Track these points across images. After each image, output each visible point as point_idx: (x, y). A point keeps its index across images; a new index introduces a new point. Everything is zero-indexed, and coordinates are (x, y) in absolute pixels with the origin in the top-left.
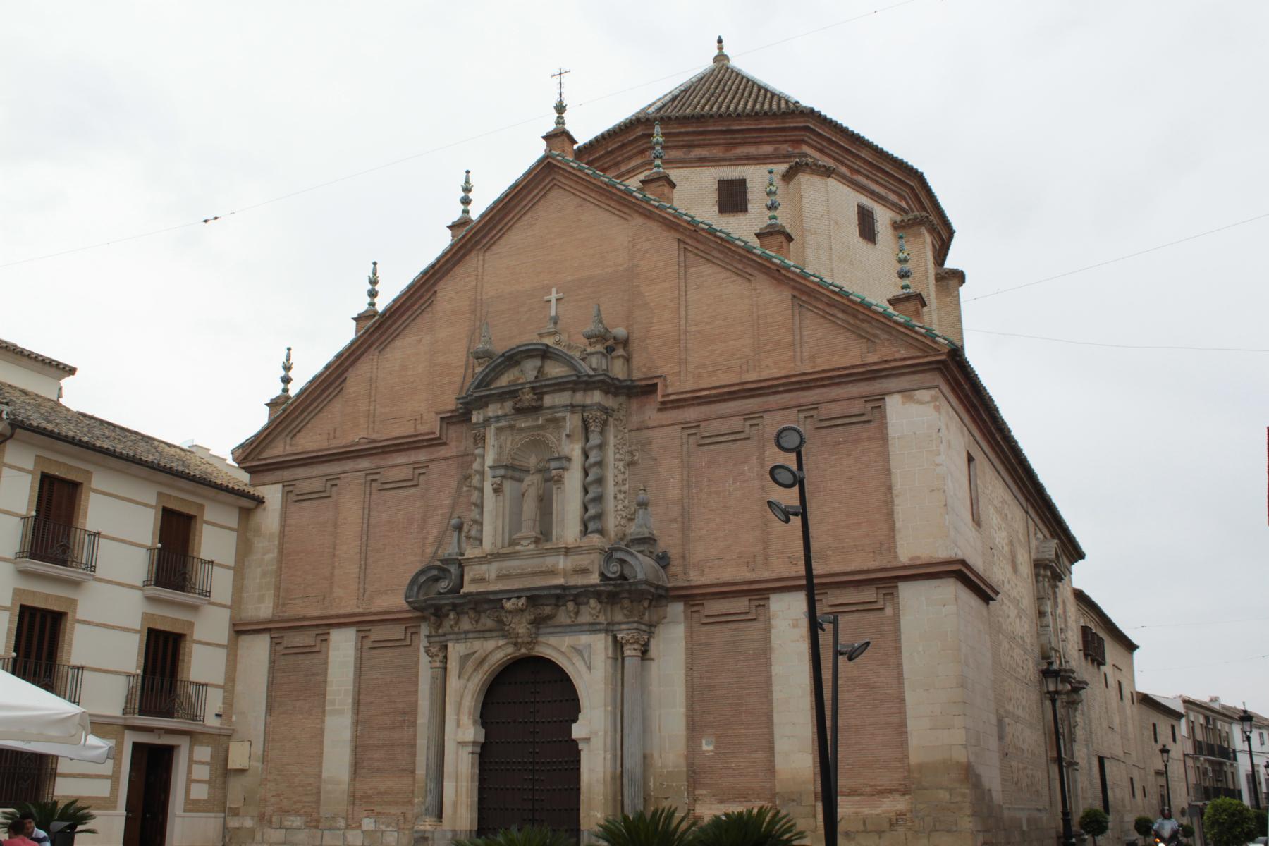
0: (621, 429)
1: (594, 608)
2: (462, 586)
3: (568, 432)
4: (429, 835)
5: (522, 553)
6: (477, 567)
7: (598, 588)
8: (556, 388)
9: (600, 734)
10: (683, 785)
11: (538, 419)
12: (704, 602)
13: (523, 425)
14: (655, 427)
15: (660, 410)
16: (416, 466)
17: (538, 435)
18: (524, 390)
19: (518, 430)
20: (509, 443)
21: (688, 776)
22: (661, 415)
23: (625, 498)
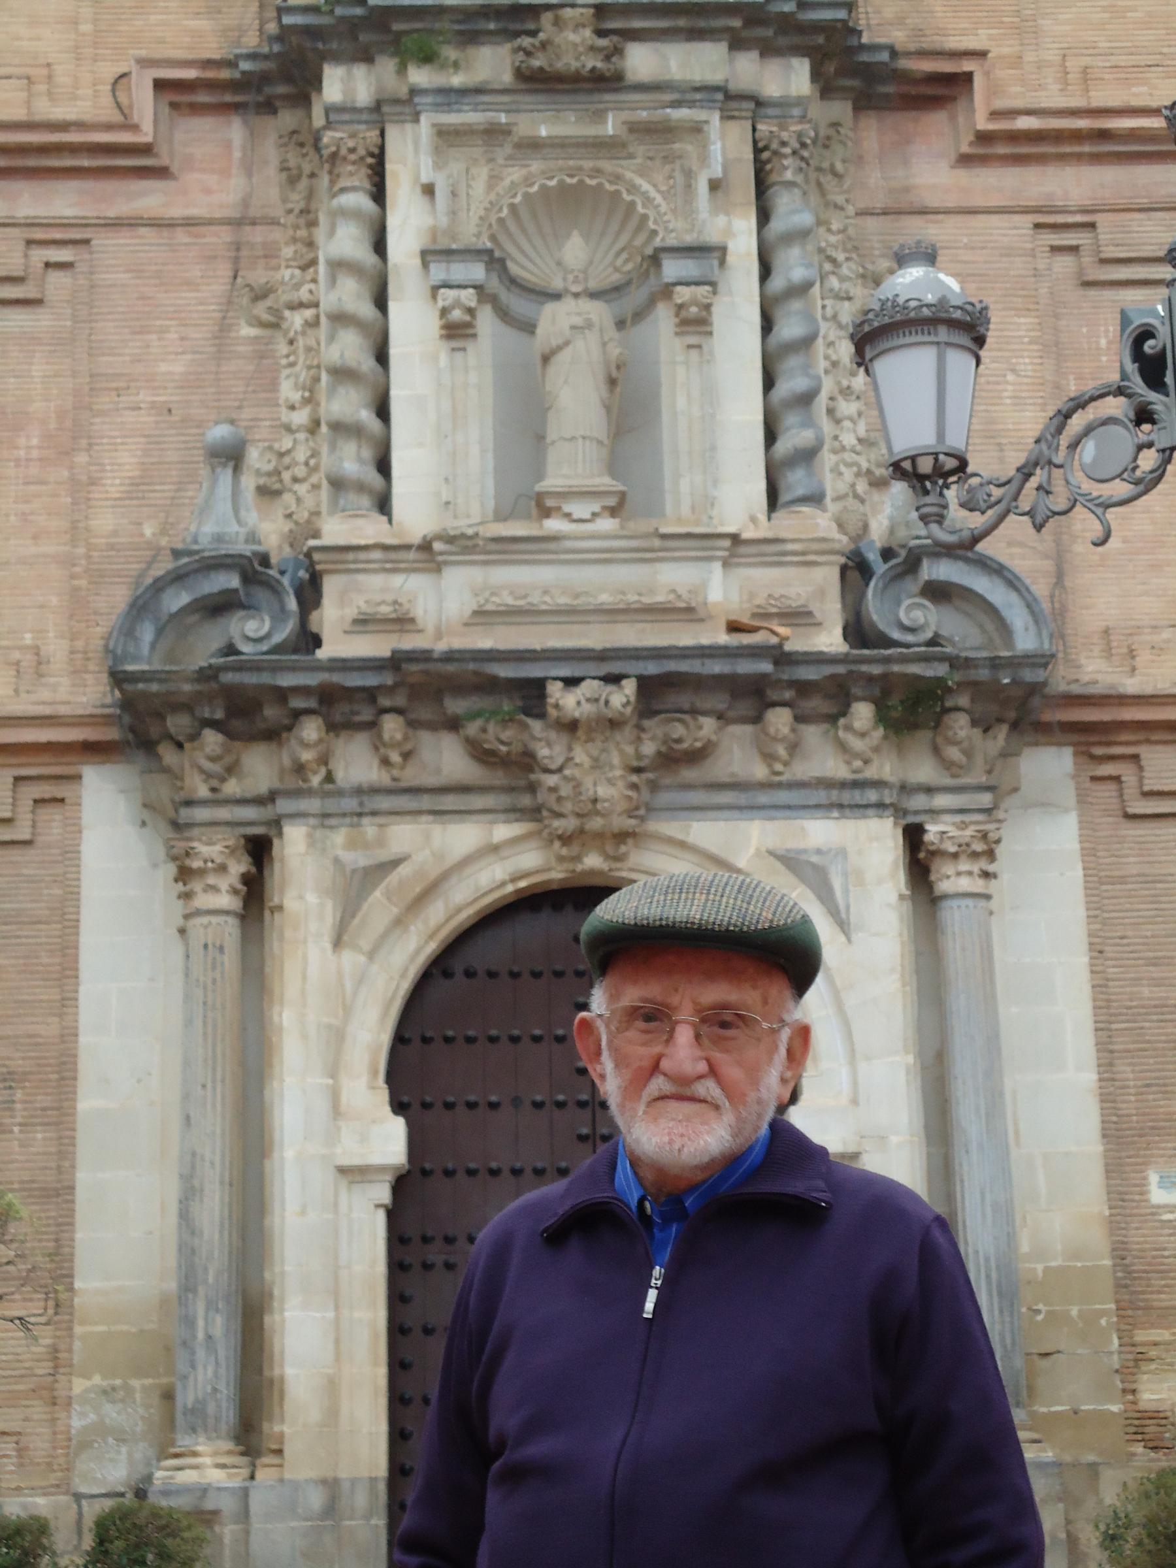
0: (840, 199)
1: (863, 735)
2: (317, 641)
3: (717, 171)
4: (227, 1504)
5: (569, 544)
6: (375, 581)
7: (896, 668)
8: (682, 22)
9: (894, 1139)
10: (1103, 1313)
11: (599, 116)
12: (1143, 751)
13: (544, 132)
14: (947, 212)
15: (965, 160)
16: (39, 234)
17: (598, 172)
18: (568, 12)
19: (518, 146)
20: (479, 187)
21: (1119, 1286)
22: (964, 176)
23: (860, 414)
